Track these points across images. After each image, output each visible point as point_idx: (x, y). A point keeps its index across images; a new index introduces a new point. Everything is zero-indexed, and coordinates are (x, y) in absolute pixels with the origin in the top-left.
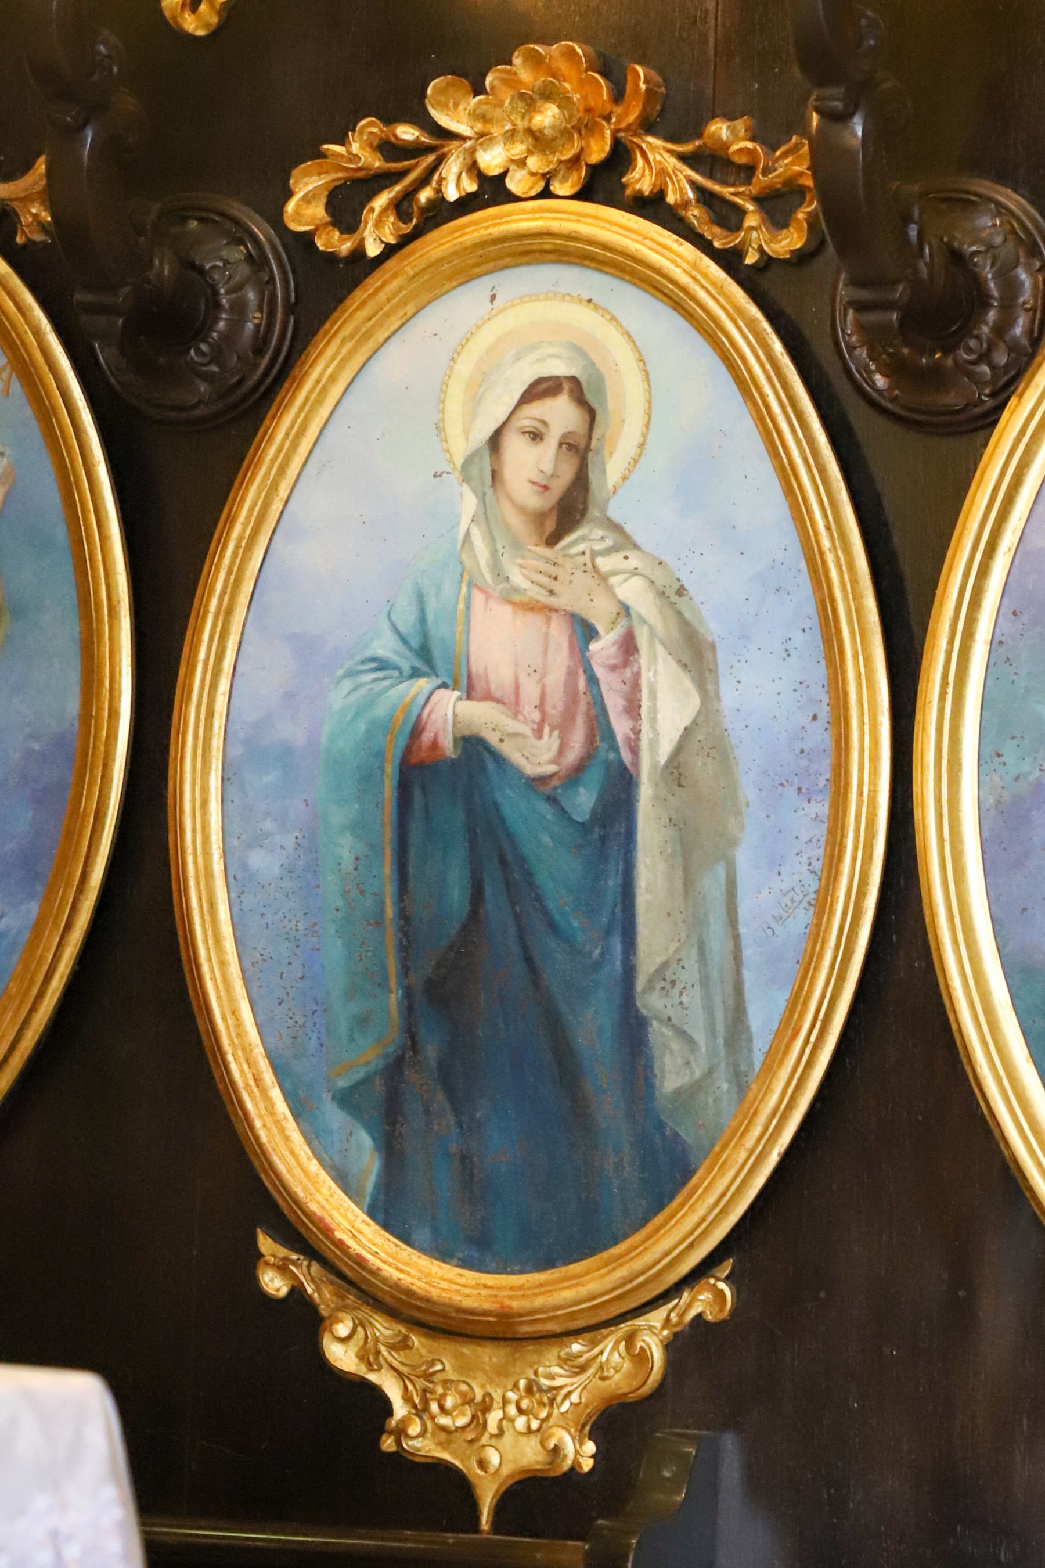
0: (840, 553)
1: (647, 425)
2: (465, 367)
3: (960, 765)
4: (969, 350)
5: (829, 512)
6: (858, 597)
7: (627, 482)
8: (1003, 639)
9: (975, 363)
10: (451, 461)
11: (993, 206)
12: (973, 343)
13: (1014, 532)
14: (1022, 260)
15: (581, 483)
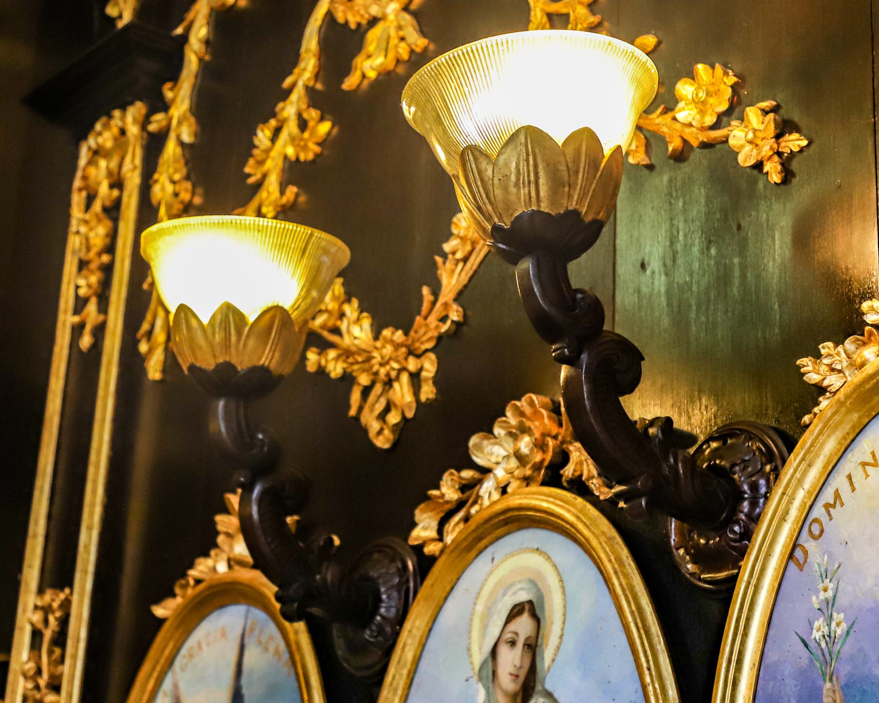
1: (564, 623)
2: (480, 608)
7: (556, 662)
10: (473, 669)
15: (533, 669)
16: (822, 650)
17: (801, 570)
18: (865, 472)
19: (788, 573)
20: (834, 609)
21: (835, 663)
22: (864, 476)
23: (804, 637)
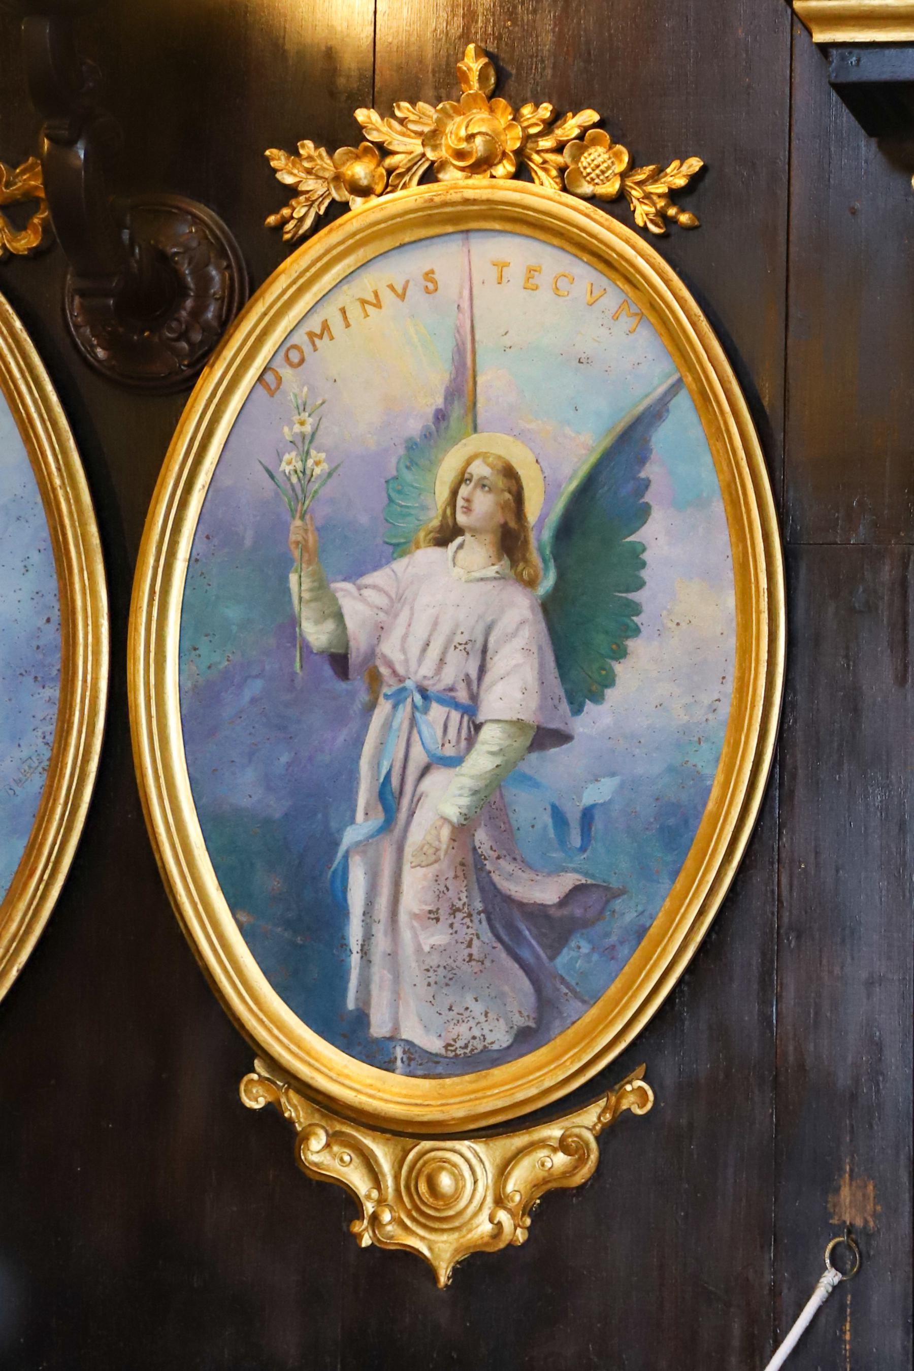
0: (68, 489)
3: (165, 657)
4: (171, 330)
5: (60, 457)
6: (83, 524)
8: (198, 557)
9: (178, 339)
11: (189, 217)
12: (174, 324)
13: (206, 474)
14: (212, 260)
16: (292, 484)
17: (272, 395)
18: (365, 310)
19: (254, 396)
20: (314, 444)
21: (311, 501)
22: (363, 315)
23: (270, 468)
